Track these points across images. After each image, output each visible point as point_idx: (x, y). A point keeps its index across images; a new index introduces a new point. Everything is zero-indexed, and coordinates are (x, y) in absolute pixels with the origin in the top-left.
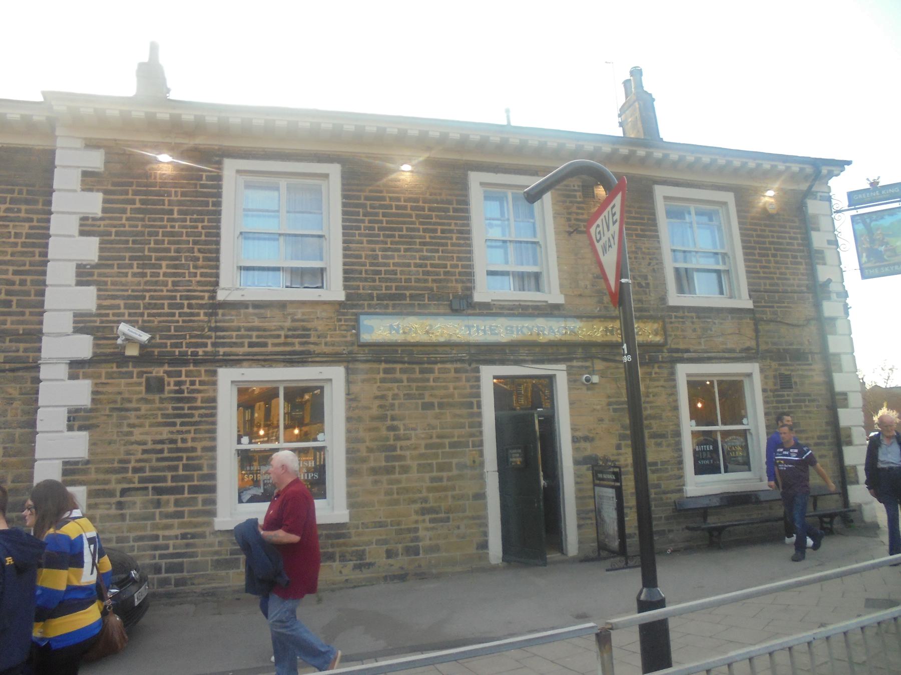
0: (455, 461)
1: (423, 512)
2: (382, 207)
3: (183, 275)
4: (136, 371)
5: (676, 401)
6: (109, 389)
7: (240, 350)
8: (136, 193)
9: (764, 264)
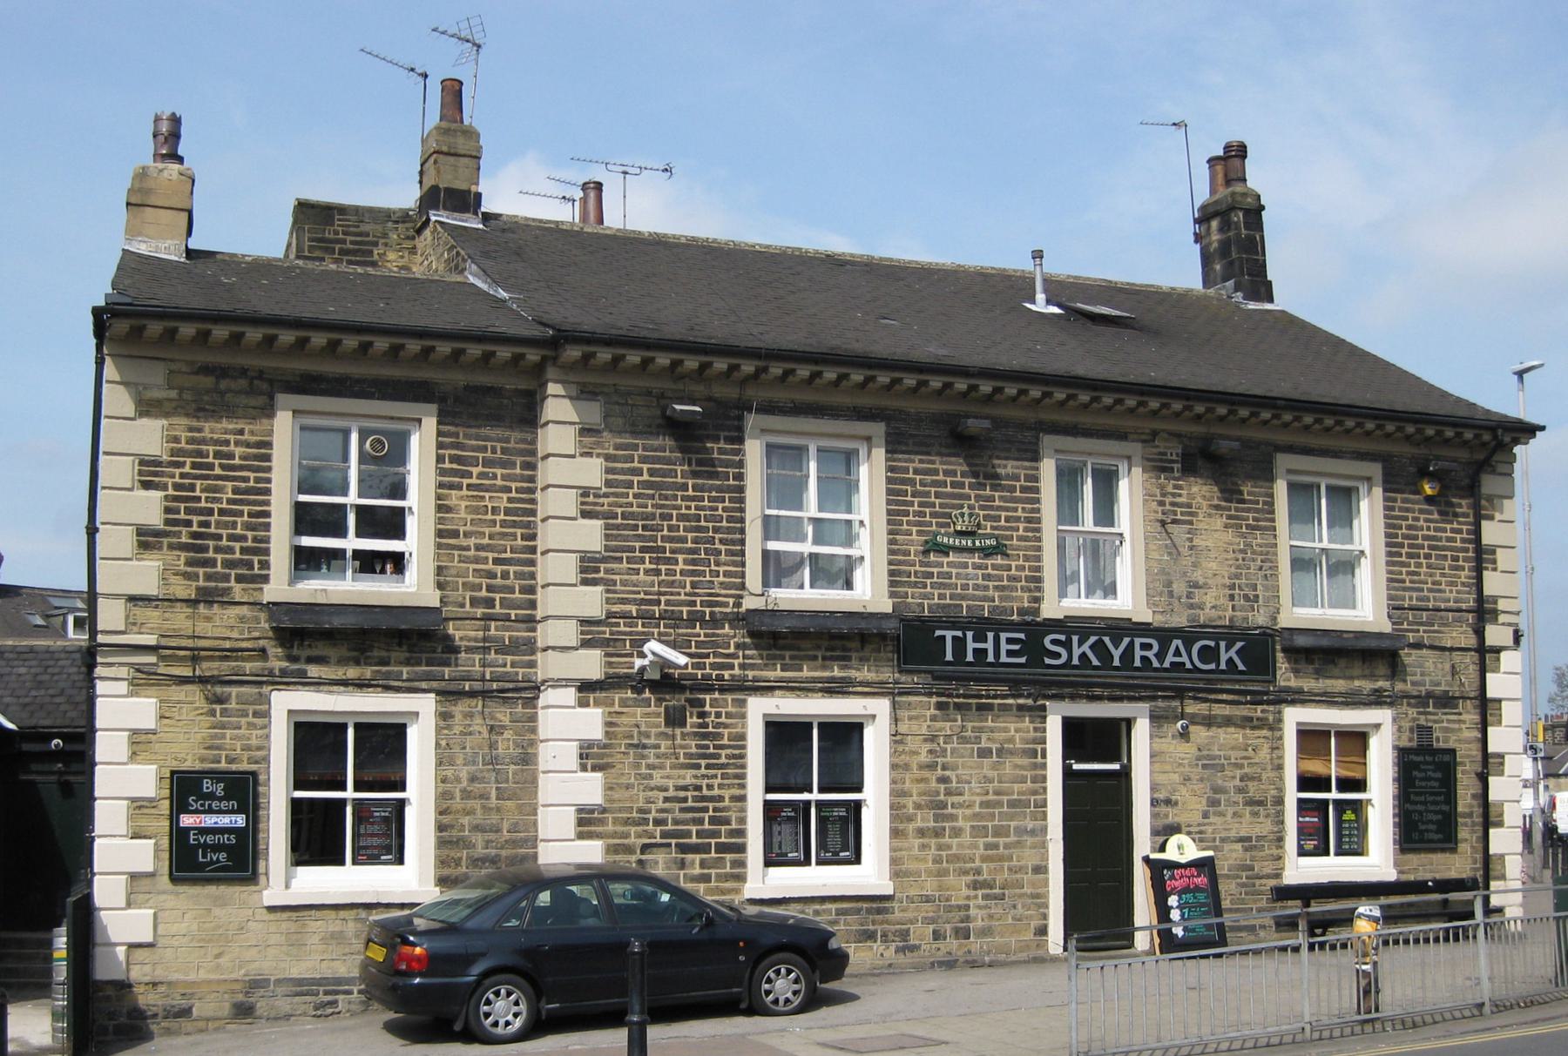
0: (1013, 824)
1: (975, 886)
2: (935, 484)
3: (703, 573)
5: (1281, 757)
6: (624, 720)
8: (643, 460)
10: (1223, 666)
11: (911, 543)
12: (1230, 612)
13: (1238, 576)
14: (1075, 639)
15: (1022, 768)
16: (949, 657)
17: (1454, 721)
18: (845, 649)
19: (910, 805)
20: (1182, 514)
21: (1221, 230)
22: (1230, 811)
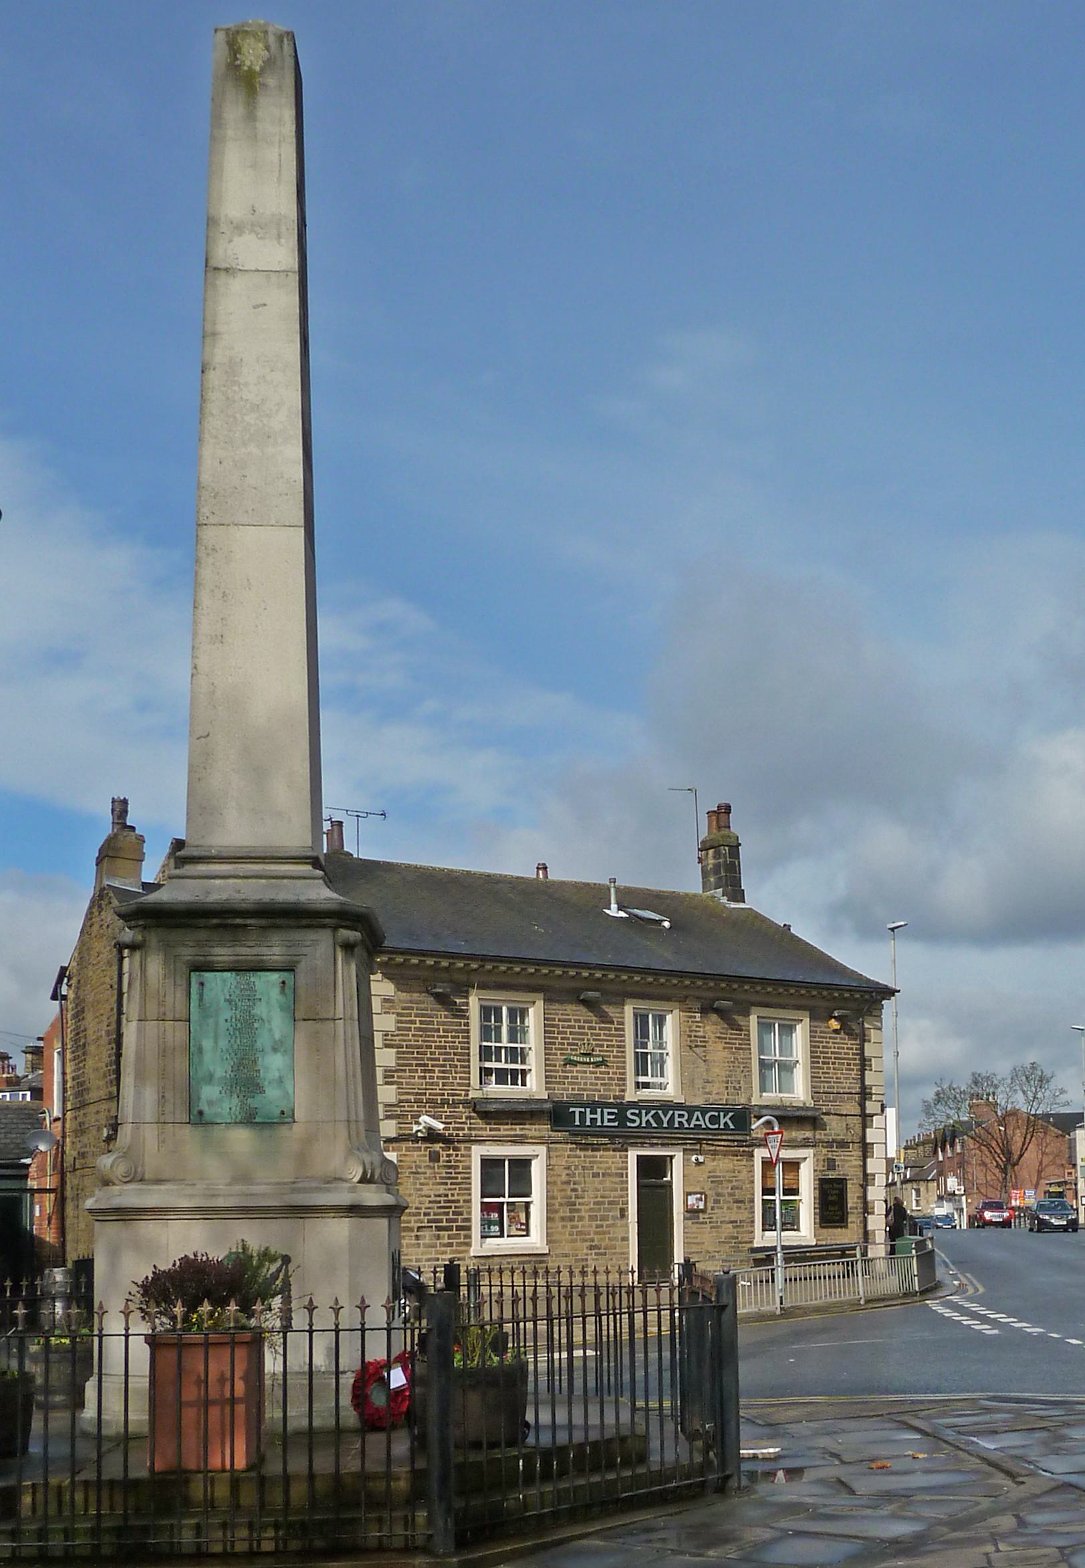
0: (611, 1214)
2: (569, 1027)
4: (423, 1146)
6: (407, 1159)
7: (484, 1133)
9: (825, 1070)
10: (722, 1127)
11: (557, 1060)
12: (726, 1096)
13: (730, 1076)
14: (644, 1112)
15: (616, 1183)
16: (577, 1123)
17: (848, 1156)
18: (524, 1119)
19: (557, 1205)
20: (701, 1042)
21: (714, 857)
22: (726, 1206)
